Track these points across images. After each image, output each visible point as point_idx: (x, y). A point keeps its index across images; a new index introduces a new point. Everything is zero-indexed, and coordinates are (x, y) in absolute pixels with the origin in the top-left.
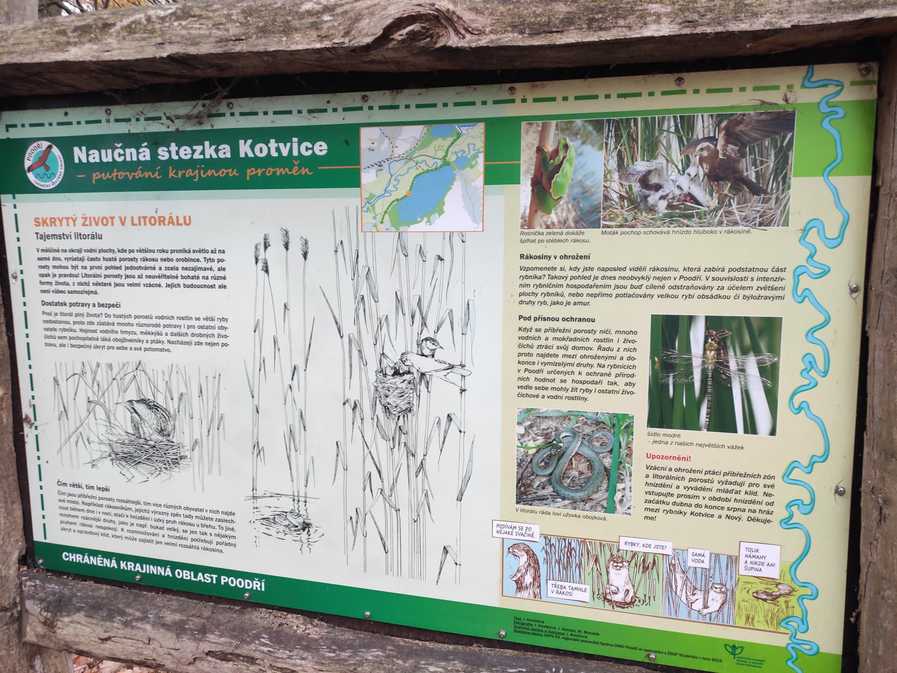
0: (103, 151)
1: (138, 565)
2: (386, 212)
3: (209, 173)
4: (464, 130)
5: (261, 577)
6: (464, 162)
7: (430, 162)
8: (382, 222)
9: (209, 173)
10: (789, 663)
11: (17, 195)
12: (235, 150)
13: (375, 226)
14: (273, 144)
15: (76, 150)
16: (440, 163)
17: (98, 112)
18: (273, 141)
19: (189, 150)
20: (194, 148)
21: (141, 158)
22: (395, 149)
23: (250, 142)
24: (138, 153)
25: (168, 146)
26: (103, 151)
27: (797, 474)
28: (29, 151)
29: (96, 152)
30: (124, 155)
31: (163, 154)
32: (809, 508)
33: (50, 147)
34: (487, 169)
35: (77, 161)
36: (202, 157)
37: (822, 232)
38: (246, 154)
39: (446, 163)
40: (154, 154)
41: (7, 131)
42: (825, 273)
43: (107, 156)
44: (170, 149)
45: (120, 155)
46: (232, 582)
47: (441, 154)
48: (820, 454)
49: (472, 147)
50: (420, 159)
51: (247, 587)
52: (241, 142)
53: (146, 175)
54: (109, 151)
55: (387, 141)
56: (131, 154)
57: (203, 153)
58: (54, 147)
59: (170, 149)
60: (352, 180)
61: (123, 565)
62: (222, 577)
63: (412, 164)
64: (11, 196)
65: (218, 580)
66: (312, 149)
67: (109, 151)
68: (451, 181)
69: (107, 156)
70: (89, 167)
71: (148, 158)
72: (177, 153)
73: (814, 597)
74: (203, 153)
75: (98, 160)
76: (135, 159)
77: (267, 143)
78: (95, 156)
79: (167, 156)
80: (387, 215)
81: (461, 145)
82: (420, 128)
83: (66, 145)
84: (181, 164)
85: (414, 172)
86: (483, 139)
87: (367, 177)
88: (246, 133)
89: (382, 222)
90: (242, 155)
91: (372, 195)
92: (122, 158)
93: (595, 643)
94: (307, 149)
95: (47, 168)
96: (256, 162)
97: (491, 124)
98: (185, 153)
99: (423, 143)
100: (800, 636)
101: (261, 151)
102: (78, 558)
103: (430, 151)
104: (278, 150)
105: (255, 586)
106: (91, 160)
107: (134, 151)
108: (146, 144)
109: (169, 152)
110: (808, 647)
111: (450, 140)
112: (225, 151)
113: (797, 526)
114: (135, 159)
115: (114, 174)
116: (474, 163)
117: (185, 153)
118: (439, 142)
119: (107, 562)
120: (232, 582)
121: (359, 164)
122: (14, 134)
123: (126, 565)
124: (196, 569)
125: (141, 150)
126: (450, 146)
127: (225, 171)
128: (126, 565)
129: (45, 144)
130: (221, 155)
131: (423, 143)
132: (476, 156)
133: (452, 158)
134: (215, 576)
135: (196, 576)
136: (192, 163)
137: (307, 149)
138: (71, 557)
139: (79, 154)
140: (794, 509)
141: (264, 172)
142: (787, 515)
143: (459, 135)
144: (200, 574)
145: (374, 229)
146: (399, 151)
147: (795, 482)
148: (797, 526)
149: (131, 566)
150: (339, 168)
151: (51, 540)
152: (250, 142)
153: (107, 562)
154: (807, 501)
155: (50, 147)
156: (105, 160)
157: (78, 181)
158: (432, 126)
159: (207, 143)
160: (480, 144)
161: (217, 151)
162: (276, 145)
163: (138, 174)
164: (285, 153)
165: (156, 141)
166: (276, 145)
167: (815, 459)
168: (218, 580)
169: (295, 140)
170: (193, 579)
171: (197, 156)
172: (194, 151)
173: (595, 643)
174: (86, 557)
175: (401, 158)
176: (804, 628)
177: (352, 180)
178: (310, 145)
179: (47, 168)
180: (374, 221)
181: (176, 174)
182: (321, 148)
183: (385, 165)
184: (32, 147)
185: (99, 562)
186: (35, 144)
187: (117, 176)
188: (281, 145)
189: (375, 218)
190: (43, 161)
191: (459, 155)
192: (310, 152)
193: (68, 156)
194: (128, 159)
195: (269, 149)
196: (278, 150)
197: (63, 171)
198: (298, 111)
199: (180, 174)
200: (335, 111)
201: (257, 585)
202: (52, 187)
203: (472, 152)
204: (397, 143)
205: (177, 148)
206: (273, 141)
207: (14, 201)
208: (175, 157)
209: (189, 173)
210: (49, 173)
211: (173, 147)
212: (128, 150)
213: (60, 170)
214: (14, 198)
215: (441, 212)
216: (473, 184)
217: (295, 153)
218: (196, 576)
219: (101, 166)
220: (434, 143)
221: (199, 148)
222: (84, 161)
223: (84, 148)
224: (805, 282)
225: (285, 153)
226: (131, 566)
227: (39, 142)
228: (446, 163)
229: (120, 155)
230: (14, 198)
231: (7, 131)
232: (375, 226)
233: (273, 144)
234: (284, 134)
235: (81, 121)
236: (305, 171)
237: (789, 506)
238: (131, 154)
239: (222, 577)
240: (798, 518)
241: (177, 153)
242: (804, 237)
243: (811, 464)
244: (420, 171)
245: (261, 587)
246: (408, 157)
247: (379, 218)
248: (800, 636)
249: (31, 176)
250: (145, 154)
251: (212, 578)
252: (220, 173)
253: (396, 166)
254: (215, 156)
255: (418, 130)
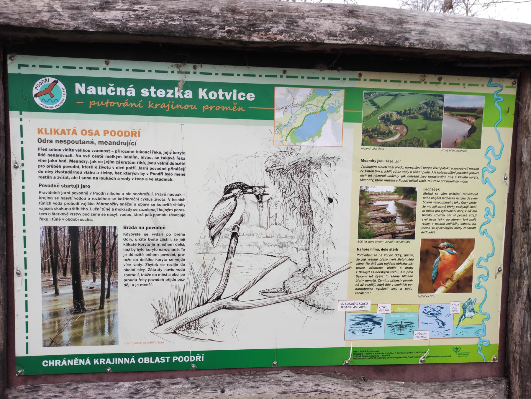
0: (99, 88)
1: (108, 359)
2: (288, 135)
3: (177, 107)
4: (333, 92)
5: (201, 353)
6: (333, 110)
7: (315, 108)
8: (286, 140)
9: (177, 107)
10: (479, 352)
11: (23, 112)
12: (196, 94)
13: (282, 142)
14: (221, 92)
15: (77, 85)
16: (320, 109)
17: (100, 63)
18: (221, 91)
19: (164, 92)
20: (168, 91)
21: (128, 94)
22: (295, 100)
23: (205, 90)
24: (126, 91)
25: (149, 88)
26: (99, 88)
27: (482, 263)
28: (37, 83)
29: (94, 88)
30: (116, 91)
31: (145, 93)
32: (486, 278)
33: (55, 82)
34: (345, 114)
35: (77, 92)
36: (172, 96)
37: (493, 152)
38: (203, 96)
39: (323, 109)
40: (138, 92)
41: (19, 68)
42: (494, 171)
43: (102, 91)
44: (150, 90)
45: (112, 91)
46: (181, 359)
47: (320, 104)
48: (491, 253)
49: (337, 102)
50: (308, 106)
51: (191, 361)
52: (200, 90)
53: (131, 105)
54: (104, 88)
55: (290, 95)
56: (121, 91)
57: (173, 94)
58: (59, 82)
59: (150, 90)
60: (269, 116)
61: (96, 361)
62: (174, 357)
63: (304, 109)
64: (19, 112)
65: (171, 360)
66: (246, 96)
67: (104, 88)
68: (326, 119)
69: (102, 91)
70: (87, 97)
71: (133, 94)
72: (155, 93)
73: (488, 319)
74: (173, 94)
75: (94, 93)
76: (123, 94)
77: (217, 91)
78: (92, 91)
79: (147, 94)
80: (289, 136)
81: (331, 100)
82: (310, 89)
83: (69, 82)
84: (157, 100)
85: (305, 113)
86: (343, 98)
87: (278, 115)
88: (203, 85)
89: (286, 140)
90: (200, 97)
91: (280, 125)
92: (114, 93)
93: (393, 358)
94: (242, 96)
95: (52, 96)
96: (209, 102)
97: (348, 91)
98: (161, 93)
99: (311, 98)
100: (483, 338)
101: (213, 95)
102: (58, 363)
103: (314, 102)
104: (224, 95)
105: (197, 359)
106: (89, 92)
107: (123, 89)
108: (132, 85)
109: (150, 92)
110: (486, 343)
111: (326, 97)
112: (189, 94)
113: (482, 287)
114: (123, 94)
115: (107, 103)
116: (338, 110)
117: (161, 93)
118: (320, 98)
119: (82, 362)
120: (181, 359)
121: (273, 106)
122: (24, 71)
123: (99, 361)
124: (153, 355)
125: (128, 89)
126: (325, 101)
127: (188, 106)
128: (99, 361)
129: (52, 80)
130: (186, 96)
131: (311, 98)
132: (339, 107)
133: (326, 107)
134: (168, 358)
135: (154, 360)
136: (165, 100)
137: (242, 96)
138: (50, 363)
139: (80, 88)
140: (481, 279)
141: (214, 109)
142: (478, 282)
143: (331, 95)
144: (157, 358)
145: (281, 144)
146: (296, 102)
147: (482, 267)
148: (482, 287)
149: (102, 361)
150: (261, 108)
151: (32, 353)
152: (205, 90)
153: (82, 362)
154: (486, 275)
155: (55, 82)
156: (100, 93)
157: (75, 105)
158: (316, 89)
159: (176, 89)
160: (342, 101)
161: (183, 94)
162: (223, 93)
163: (125, 104)
164: (228, 98)
165: (139, 84)
166: (223, 93)
167: (489, 255)
168: (171, 360)
169: (235, 91)
170: (151, 362)
171: (169, 96)
172: (167, 93)
173: (393, 358)
174: (64, 361)
175: (298, 105)
176: (484, 334)
177: (269, 116)
178: (244, 94)
179: (52, 96)
180: (281, 139)
181: (154, 105)
182: (251, 97)
183: (289, 109)
184: (40, 81)
185: (75, 362)
186: (44, 79)
187: (109, 104)
188: (226, 93)
189: (282, 137)
190: (48, 91)
191: (331, 105)
192: (244, 99)
193: (70, 89)
194: (118, 94)
195: (218, 95)
196: (224, 95)
197: (65, 98)
198: (238, 75)
199: (156, 106)
200: (260, 76)
201: (198, 358)
202: (55, 108)
203: (337, 105)
204: (296, 97)
205: (155, 90)
206: (221, 91)
207: (21, 116)
208: (153, 95)
209: (163, 106)
210: (53, 99)
211: (153, 89)
212: (118, 89)
213: (62, 97)
214: (21, 114)
215: (320, 136)
216: (337, 122)
217: (235, 98)
218: (154, 360)
219: (97, 97)
220: (317, 98)
221: (171, 91)
222: (83, 92)
223: (84, 85)
224: (487, 174)
225: (228, 98)
226: (102, 361)
227: (47, 78)
228: (323, 109)
229: (112, 91)
230: (21, 114)
231: (19, 68)
232: (282, 142)
233: (221, 92)
234: (228, 87)
235: (81, 68)
236: (240, 109)
237: (479, 278)
238: (121, 91)
239: (174, 357)
240: (483, 283)
241: (155, 93)
242: (487, 154)
243: (488, 258)
244: (309, 113)
245: (201, 359)
246: (302, 105)
247: (284, 137)
248: (483, 338)
249: (37, 100)
250: (132, 92)
251: (166, 359)
252: (185, 107)
253: (295, 110)
254: (181, 97)
255: (308, 91)
